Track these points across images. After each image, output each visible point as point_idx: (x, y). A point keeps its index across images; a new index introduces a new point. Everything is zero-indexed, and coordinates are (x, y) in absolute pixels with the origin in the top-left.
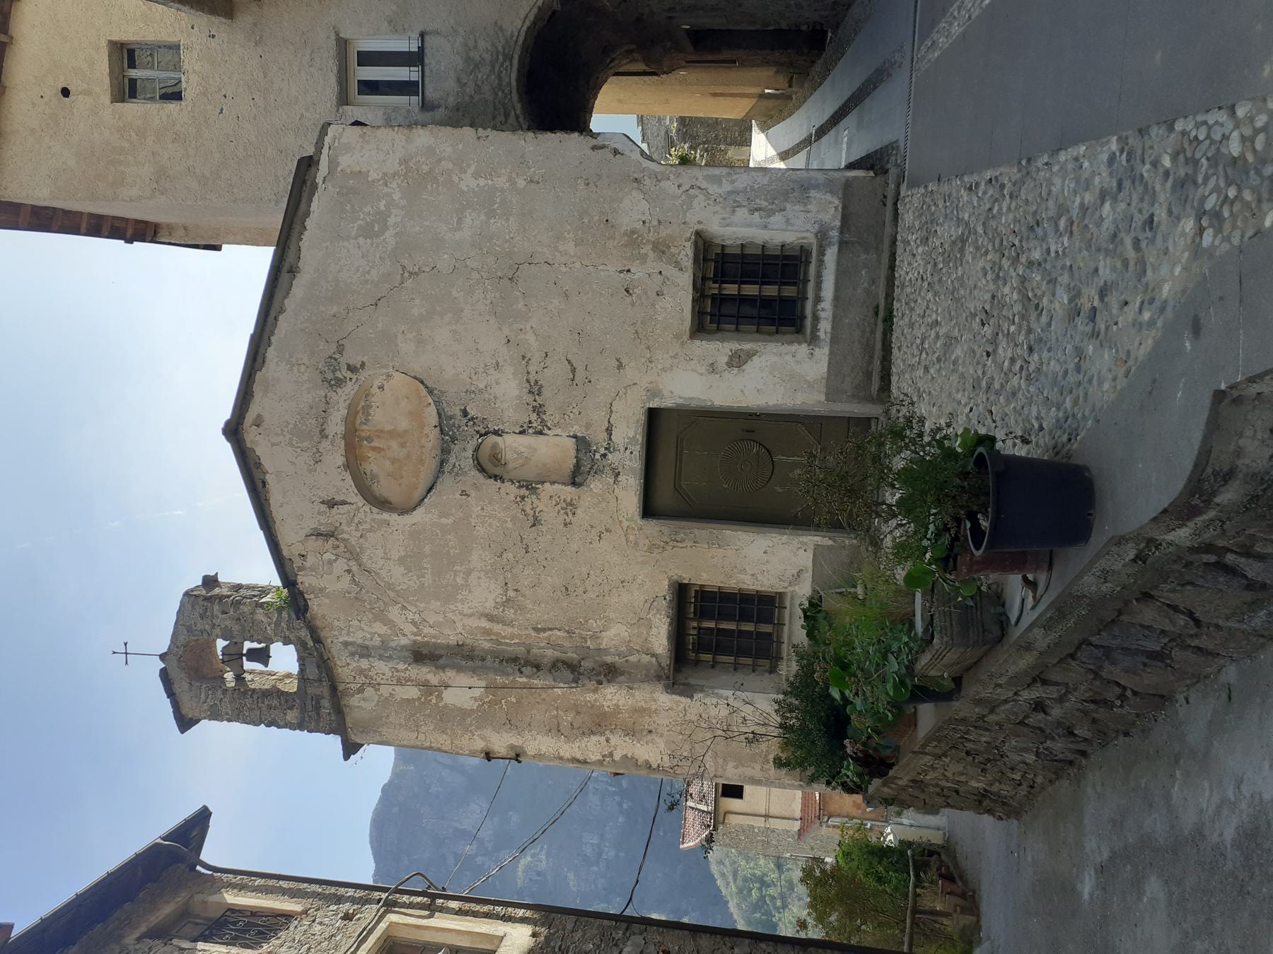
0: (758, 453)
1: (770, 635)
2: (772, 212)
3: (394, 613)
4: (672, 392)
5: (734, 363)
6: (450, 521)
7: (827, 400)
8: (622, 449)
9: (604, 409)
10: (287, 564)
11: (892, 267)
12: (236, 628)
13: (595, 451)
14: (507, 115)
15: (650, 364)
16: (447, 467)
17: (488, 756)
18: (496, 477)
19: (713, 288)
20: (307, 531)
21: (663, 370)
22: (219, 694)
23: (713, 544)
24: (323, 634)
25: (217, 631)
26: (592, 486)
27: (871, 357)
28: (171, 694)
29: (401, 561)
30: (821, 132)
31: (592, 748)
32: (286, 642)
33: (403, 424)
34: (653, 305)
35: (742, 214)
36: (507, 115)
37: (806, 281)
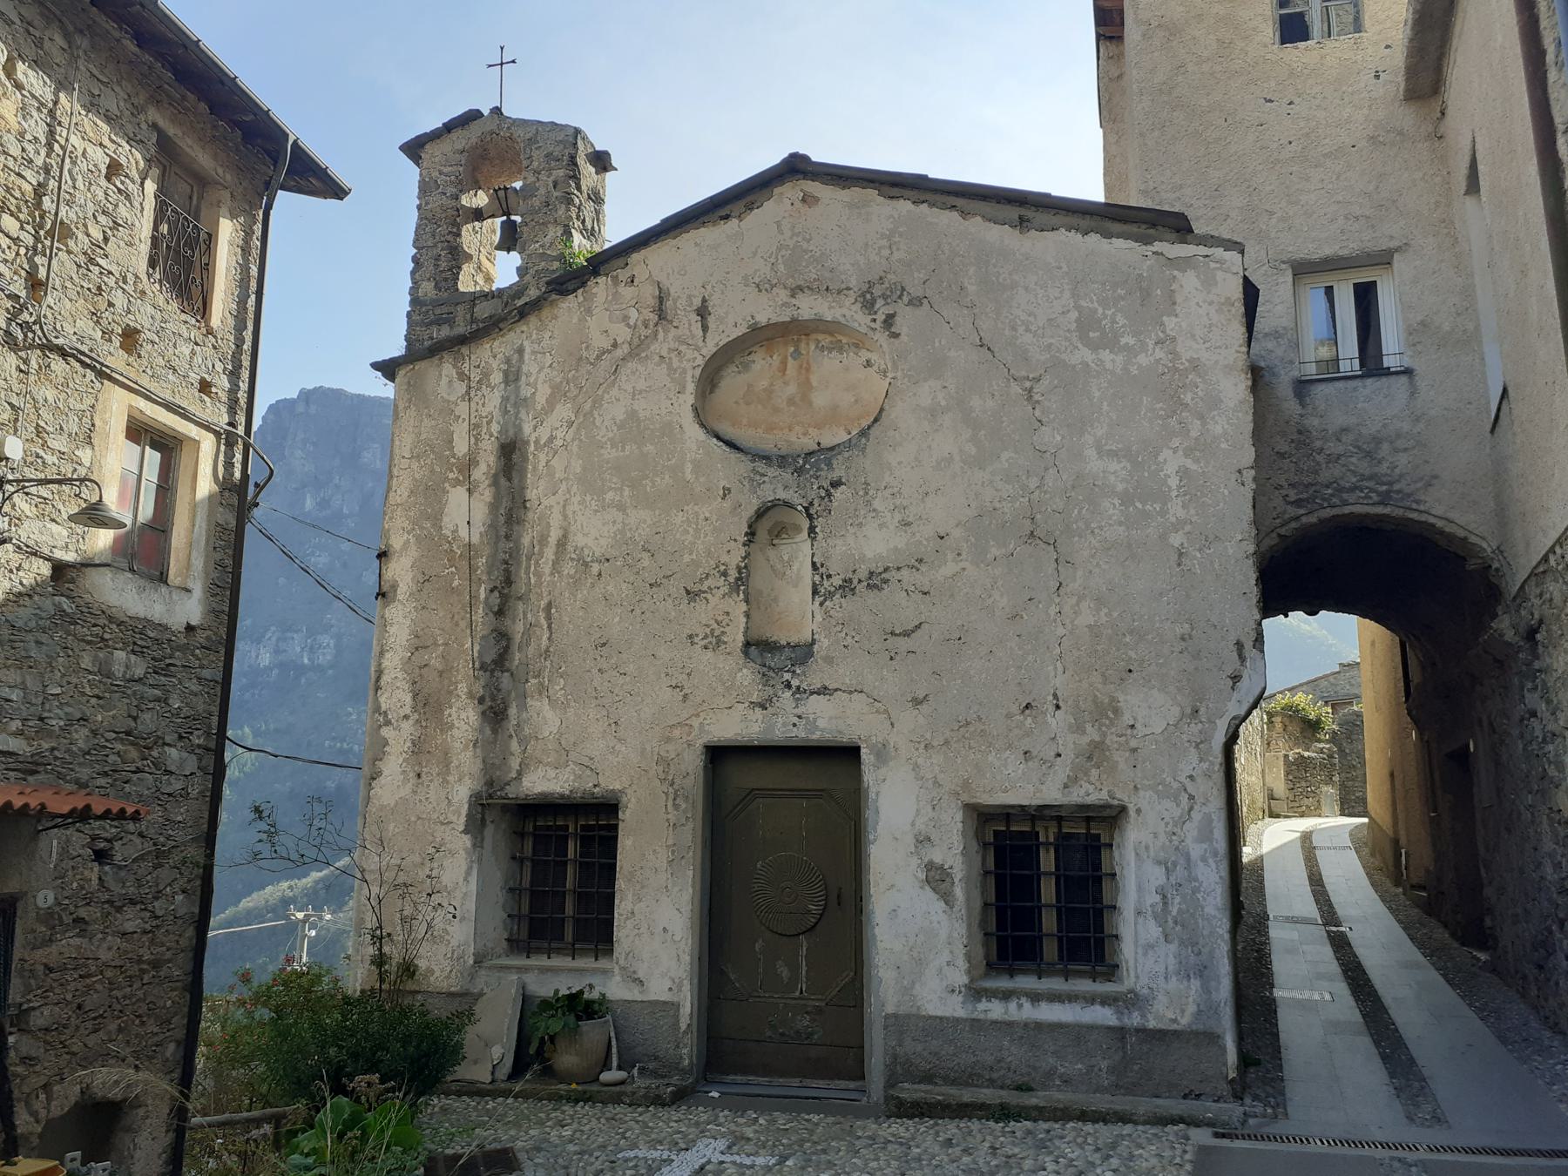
0: (809, 912)
1: (561, 938)
2: (1162, 923)
3: (564, 411)
4: (884, 780)
5: (932, 873)
6: (689, 476)
7: (887, 1017)
8: (798, 711)
9: (854, 682)
10: (621, 262)
11: (1084, 1116)
12: (536, 202)
13: (794, 672)
14: (1298, 503)
15: (923, 745)
16: (761, 466)
17: (382, 555)
18: (751, 534)
19: (1047, 834)
20: (665, 283)
21: (916, 767)
22: (451, 190)
23: (673, 852)
24: (533, 319)
25: (531, 179)
26: (745, 671)
27: (954, 1082)
28: (449, 127)
29: (632, 415)
31: (397, 697)
32: (521, 271)
33: (820, 400)
34: (1010, 747)
35: (1157, 876)
36: (1298, 503)
37: (1067, 975)
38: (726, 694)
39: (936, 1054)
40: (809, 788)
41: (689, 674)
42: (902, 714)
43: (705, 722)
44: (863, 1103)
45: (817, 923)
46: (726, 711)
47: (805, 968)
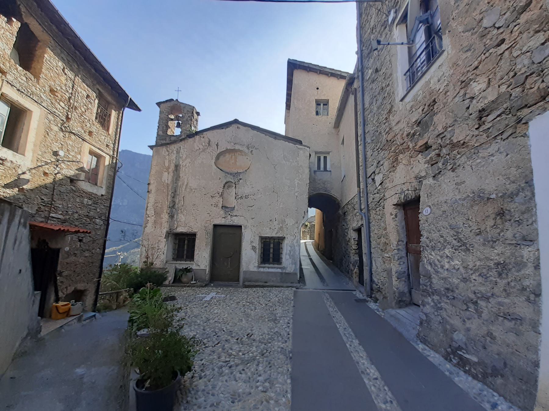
1: (183, 257)
2: (289, 256)
3: (189, 160)
6: (213, 175)
10: (202, 133)
11: (276, 287)
12: (185, 119)
16: (227, 174)
17: (149, 184)
18: (224, 186)
19: (272, 241)
20: (210, 138)
22: (167, 114)
24: (183, 142)
25: (184, 115)
27: (254, 282)
28: (167, 101)
29: (202, 162)
30: (311, 259)
31: (151, 212)
32: (181, 132)
33: (238, 164)
34: (268, 227)
35: (289, 248)
37: (273, 264)
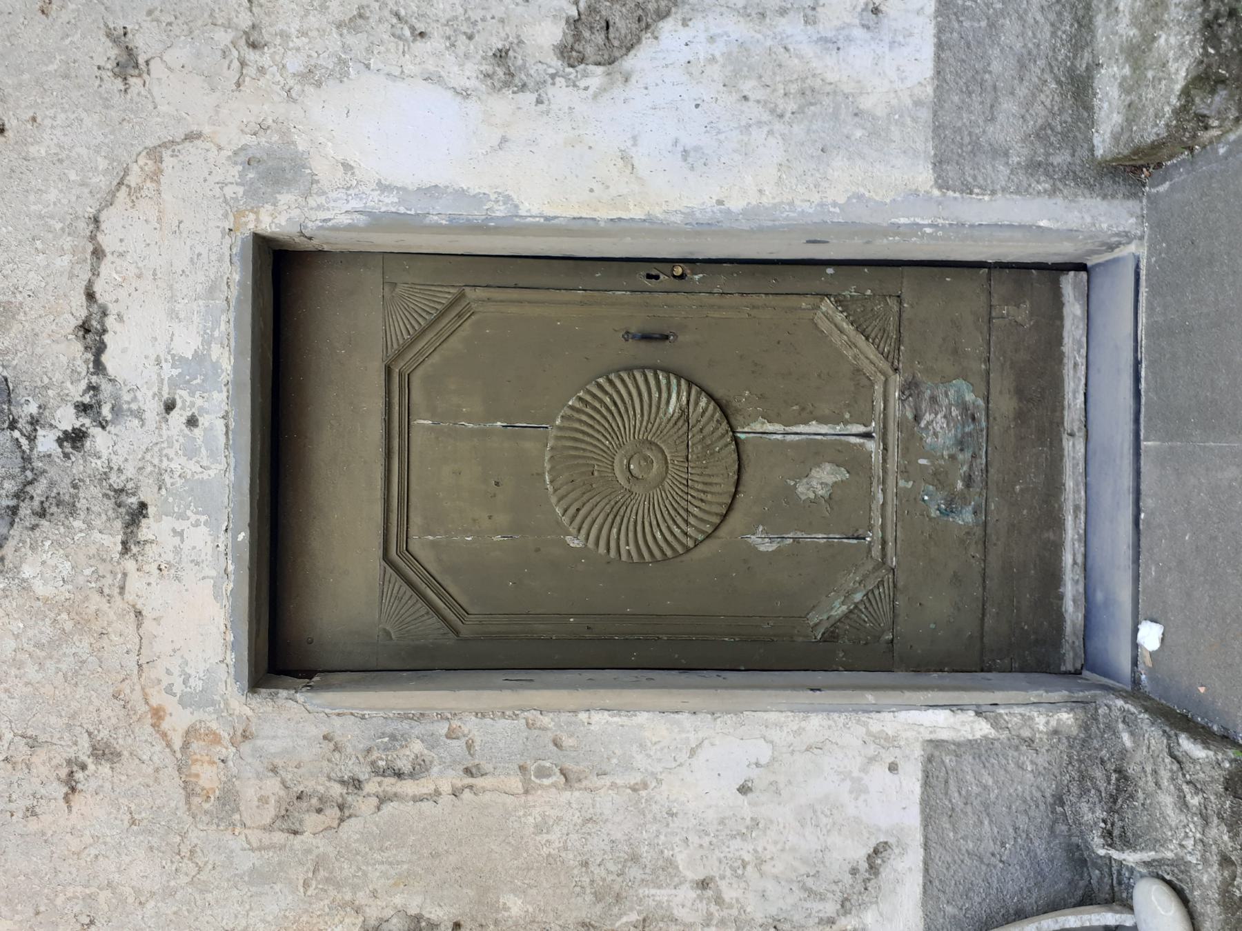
0: (684, 413)
4: (347, 167)
5: (589, 51)
7: (942, 183)
8: (153, 408)
9: (67, 242)
13: (34, 422)
15: (251, 55)
21: (310, 76)
23: (542, 773)
26: (27, 571)
38: (97, 627)
39: (1022, 66)
40: (380, 404)
41: (33, 743)
42: (163, 108)
43: (178, 688)
44: (1143, 252)
45: (711, 396)
46: (148, 625)
47: (814, 427)
